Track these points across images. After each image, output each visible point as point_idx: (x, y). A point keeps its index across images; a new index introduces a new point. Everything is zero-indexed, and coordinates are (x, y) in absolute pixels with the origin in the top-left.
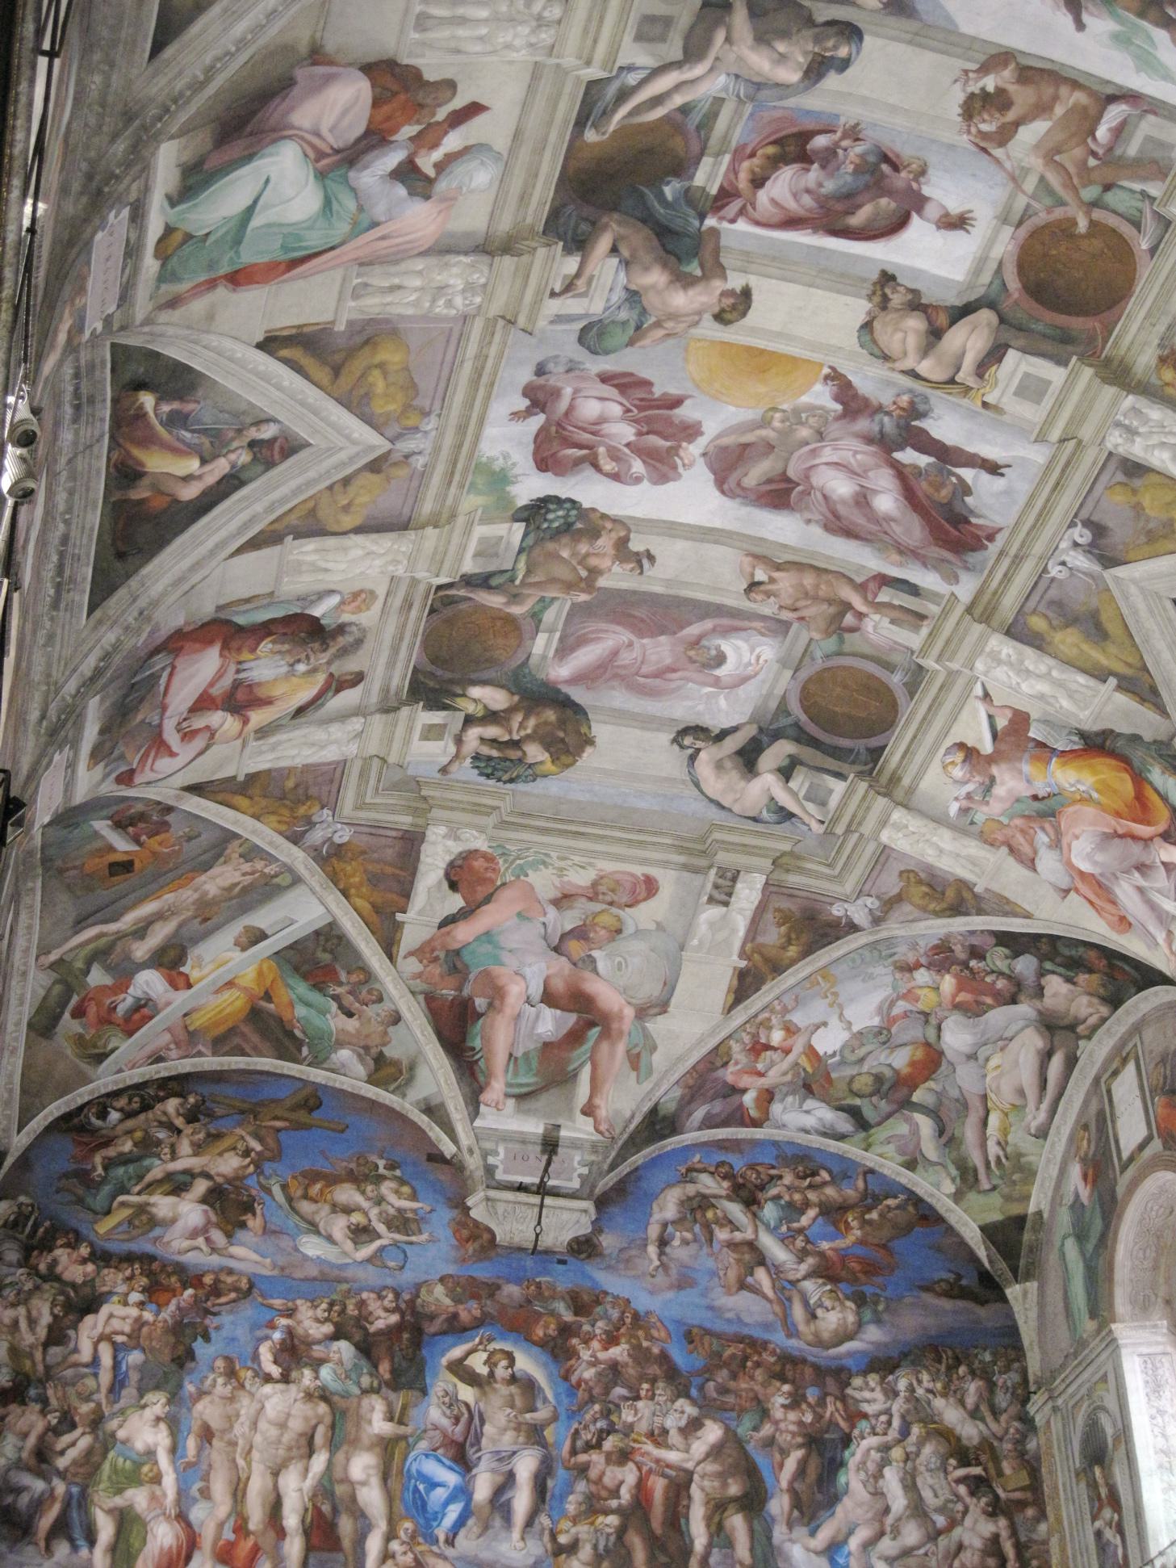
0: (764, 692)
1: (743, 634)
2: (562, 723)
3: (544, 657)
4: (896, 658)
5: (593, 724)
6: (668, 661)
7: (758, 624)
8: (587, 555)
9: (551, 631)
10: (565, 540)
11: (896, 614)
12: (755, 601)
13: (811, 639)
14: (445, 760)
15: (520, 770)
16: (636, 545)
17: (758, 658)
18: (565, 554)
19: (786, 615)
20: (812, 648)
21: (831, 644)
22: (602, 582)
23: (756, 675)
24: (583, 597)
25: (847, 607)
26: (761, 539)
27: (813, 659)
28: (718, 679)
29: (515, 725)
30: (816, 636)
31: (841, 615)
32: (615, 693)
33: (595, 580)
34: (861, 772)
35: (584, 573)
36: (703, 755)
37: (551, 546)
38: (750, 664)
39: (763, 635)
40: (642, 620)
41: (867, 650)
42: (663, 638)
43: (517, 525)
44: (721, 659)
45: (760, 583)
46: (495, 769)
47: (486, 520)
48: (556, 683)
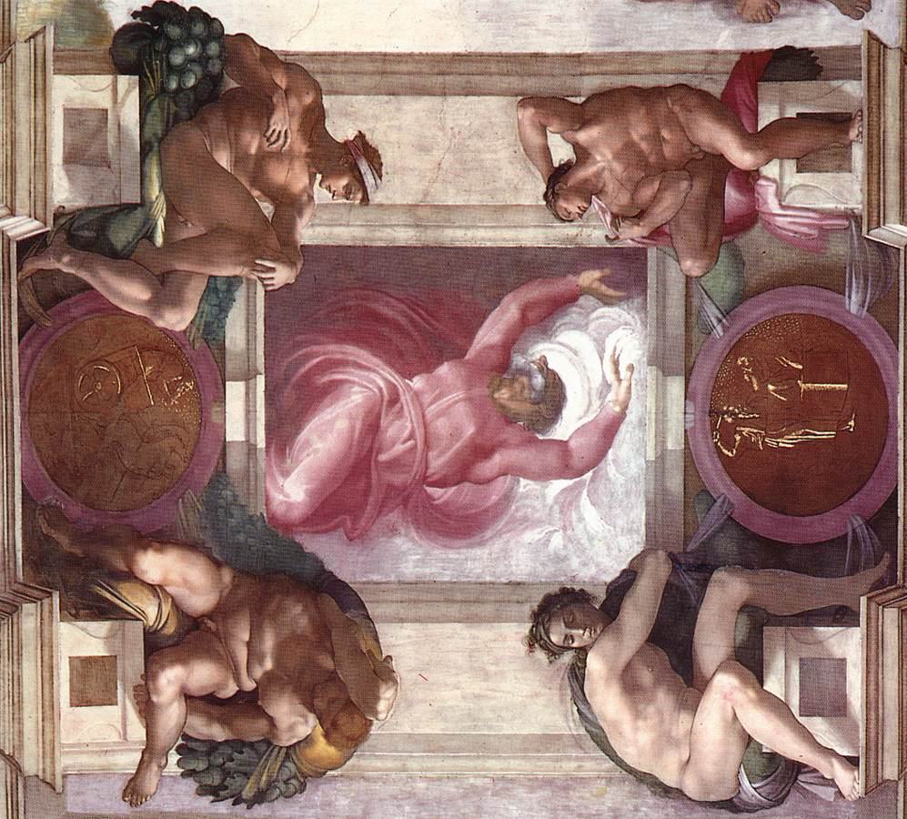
0: (651, 455)
1: (574, 314)
2: (322, 631)
3: (250, 448)
4: (839, 248)
5: (381, 628)
6: (470, 430)
7: (589, 277)
8: (263, 158)
9: (248, 376)
10: (216, 122)
11: (802, 140)
12: (566, 219)
13: (688, 279)
14: (129, 760)
15: (273, 765)
16: (341, 130)
17: (616, 363)
18: (224, 159)
19: (631, 235)
20: (695, 302)
21: (721, 282)
22: (308, 232)
23: (625, 408)
24: (282, 275)
25: (718, 166)
26: (536, 55)
27: (708, 331)
28: (563, 445)
29: (242, 654)
30: (692, 266)
31: (717, 194)
32: (401, 543)
33: (291, 228)
34: (879, 585)
35: (267, 208)
36: (595, 664)
37: (194, 135)
38: (607, 386)
39: (607, 301)
40: (399, 328)
41: (783, 258)
42: (444, 370)
43: (124, 81)
44: (553, 396)
45: (566, 168)
46: (226, 773)
47: (71, 63)
48: (288, 527)
